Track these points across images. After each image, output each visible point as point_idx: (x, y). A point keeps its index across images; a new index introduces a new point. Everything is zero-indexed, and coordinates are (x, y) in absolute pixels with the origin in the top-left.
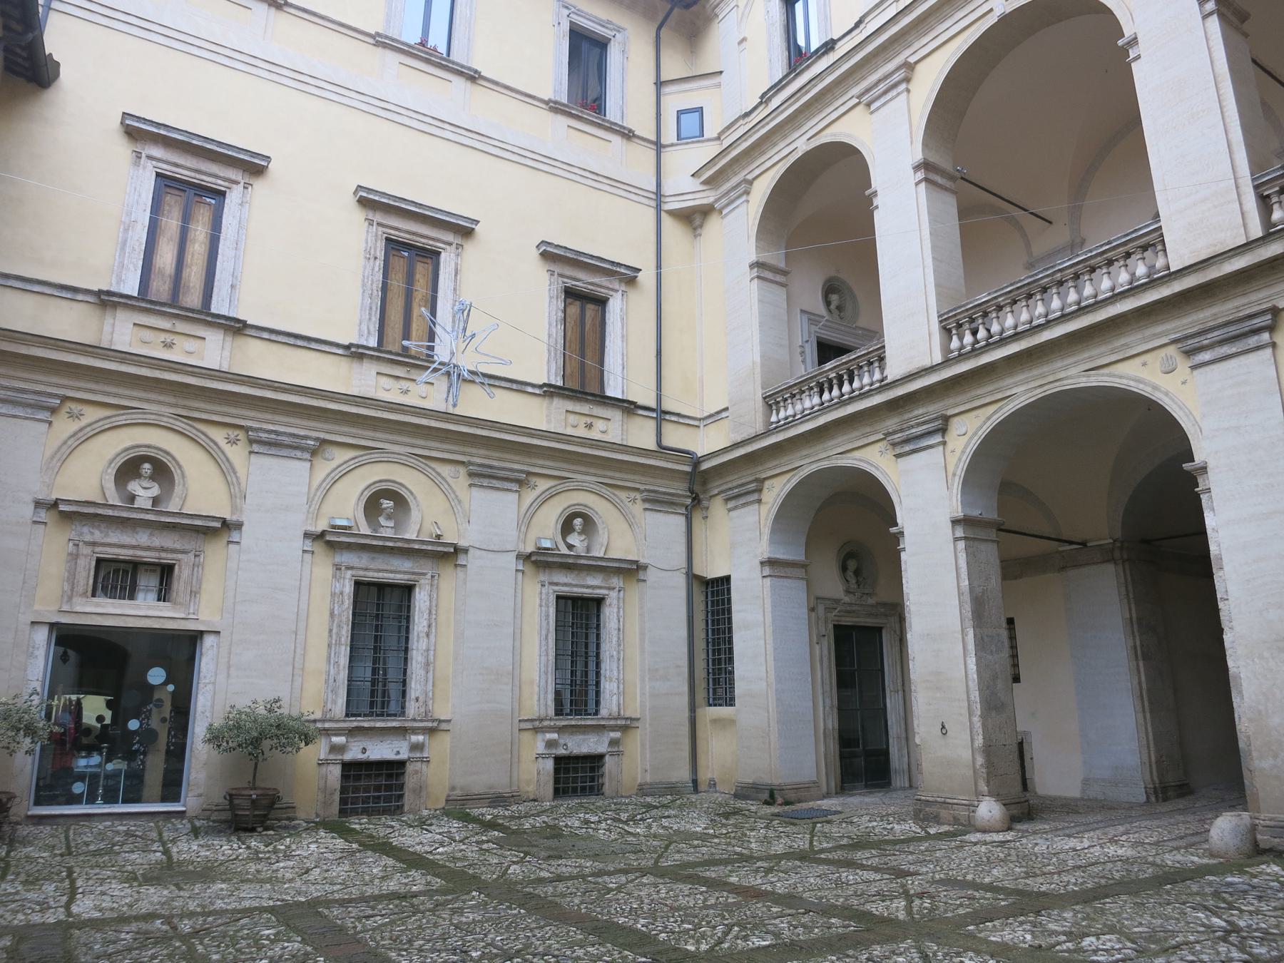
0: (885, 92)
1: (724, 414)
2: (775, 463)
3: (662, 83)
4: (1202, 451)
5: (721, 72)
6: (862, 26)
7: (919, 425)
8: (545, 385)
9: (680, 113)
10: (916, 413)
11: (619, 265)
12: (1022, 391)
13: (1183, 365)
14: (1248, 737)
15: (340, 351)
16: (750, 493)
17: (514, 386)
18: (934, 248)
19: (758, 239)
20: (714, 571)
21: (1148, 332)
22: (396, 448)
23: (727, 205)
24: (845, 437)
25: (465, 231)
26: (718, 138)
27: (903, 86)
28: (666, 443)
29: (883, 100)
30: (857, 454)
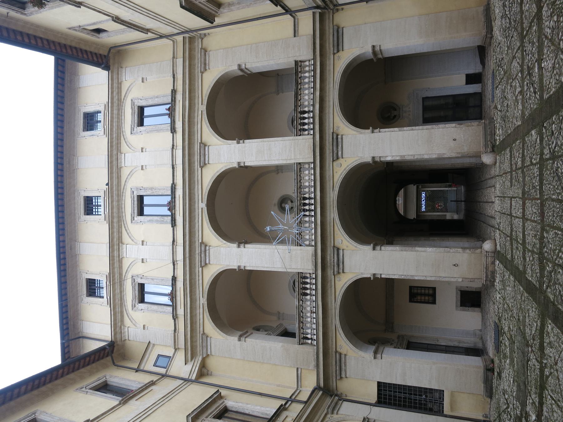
2: (330, 341)
4: (368, 159)
5: (149, 342)
7: (334, 258)
9: (155, 365)
10: (329, 260)
11: (212, 395)
12: (333, 214)
13: (341, 161)
14: (458, 153)
16: (341, 358)
19: (229, 335)
20: (373, 396)
21: (327, 168)
24: (329, 297)
26: (176, 349)
27: (207, 248)
28: (305, 399)
29: (207, 258)
30: (337, 294)
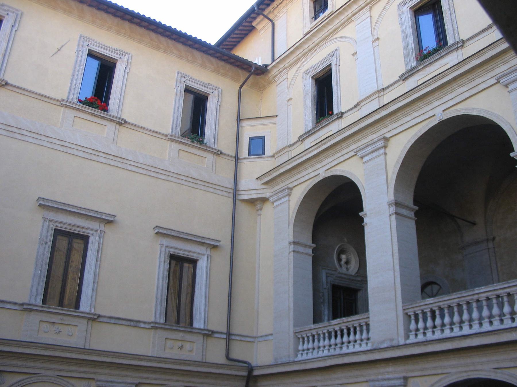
0: (372, 152)
1: (270, 338)
3: (240, 120)
5: (277, 116)
6: (359, 107)
8: (152, 322)
9: (251, 139)
15: (17, 307)
17: (132, 323)
18: (400, 259)
19: (295, 226)
22: (48, 373)
23: (277, 200)
25: (108, 221)
26: (274, 156)
27: (382, 151)
